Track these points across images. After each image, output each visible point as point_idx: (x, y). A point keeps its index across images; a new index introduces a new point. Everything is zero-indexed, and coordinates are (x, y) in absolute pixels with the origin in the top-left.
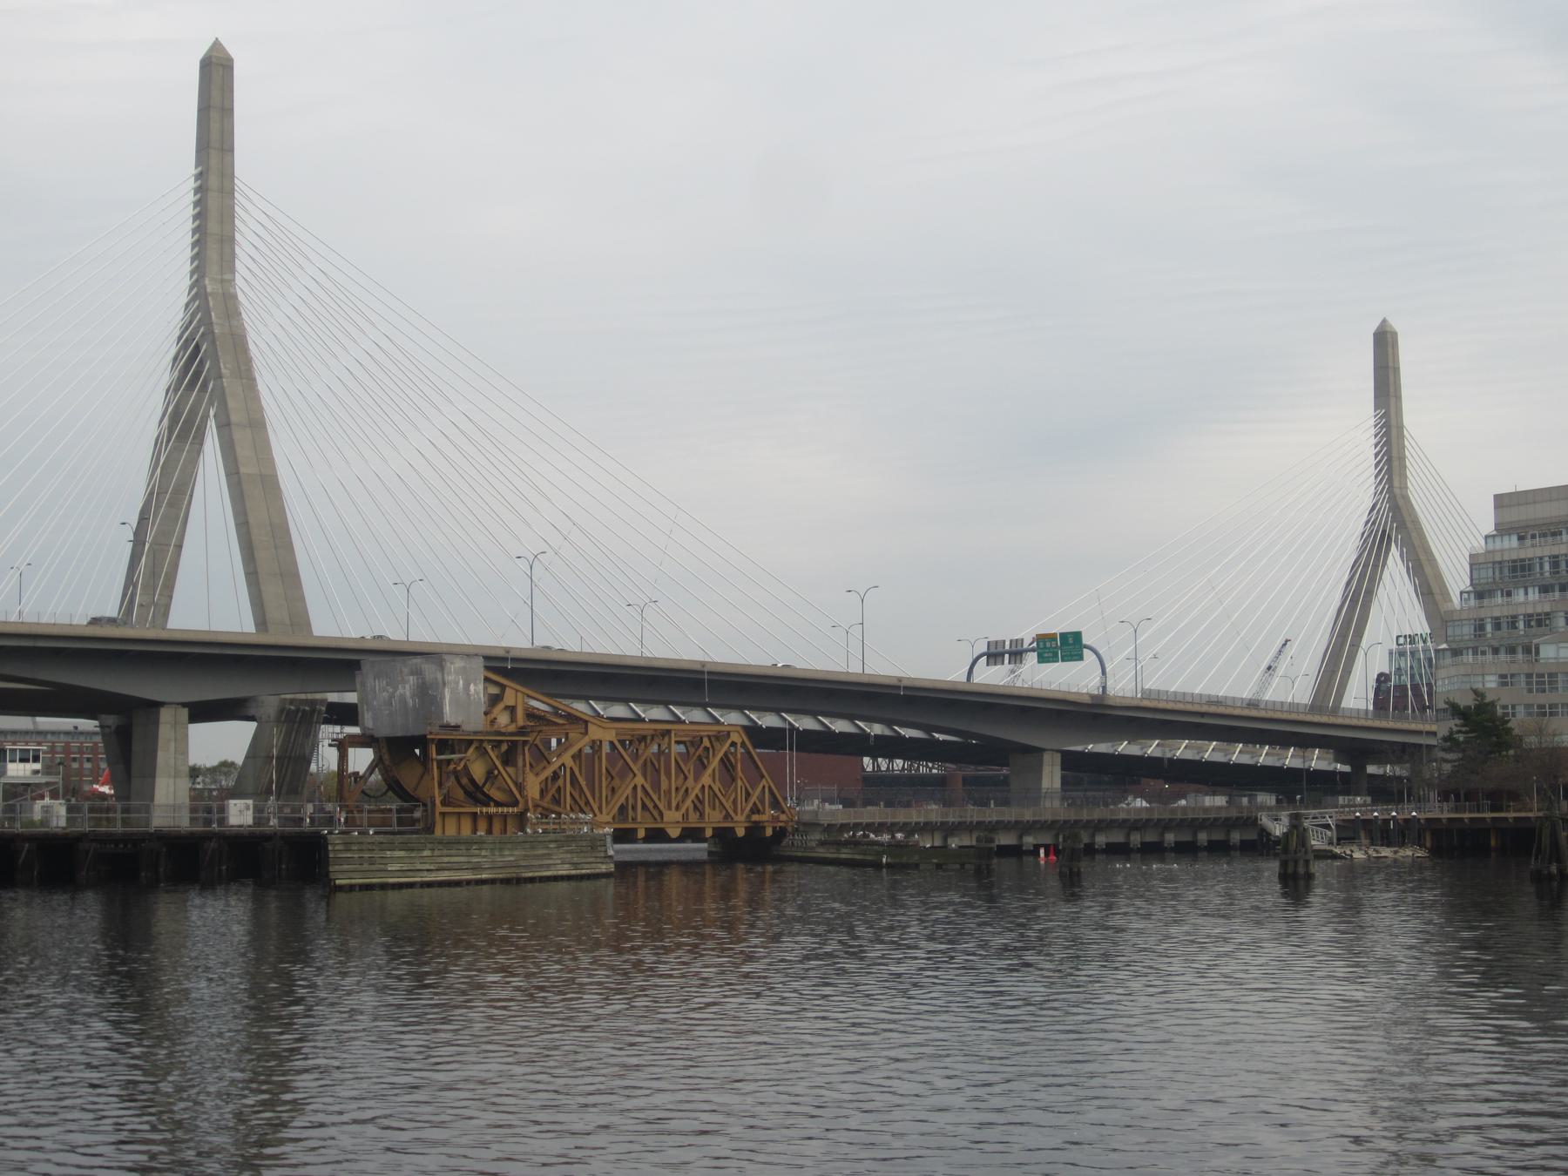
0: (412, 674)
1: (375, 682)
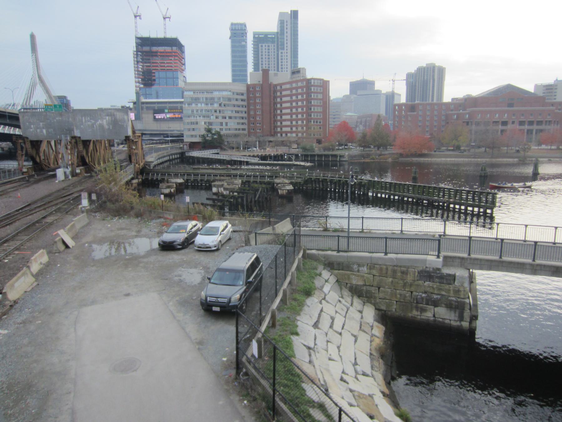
0: (108, 115)
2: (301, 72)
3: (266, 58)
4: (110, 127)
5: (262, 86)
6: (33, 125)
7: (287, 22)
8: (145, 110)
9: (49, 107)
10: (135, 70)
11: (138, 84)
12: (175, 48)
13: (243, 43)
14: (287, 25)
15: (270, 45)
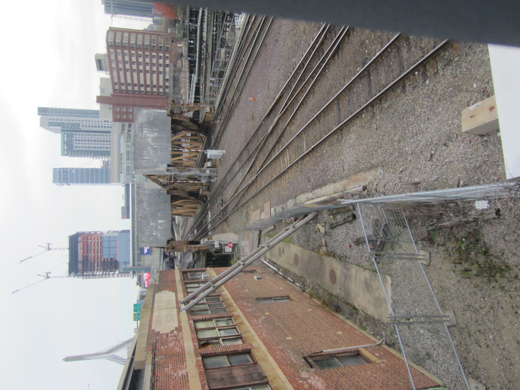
0: (142, 131)
1: (145, 159)
2: (100, 58)
3: (88, 144)
4: (155, 130)
5: (115, 105)
6: (153, 232)
7: (50, 119)
8: (140, 263)
9: (136, 316)
10: (102, 277)
11: (115, 275)
12: (80, 239)
13: (74, 171)
14: (54, 120)
15: (75, 138)
